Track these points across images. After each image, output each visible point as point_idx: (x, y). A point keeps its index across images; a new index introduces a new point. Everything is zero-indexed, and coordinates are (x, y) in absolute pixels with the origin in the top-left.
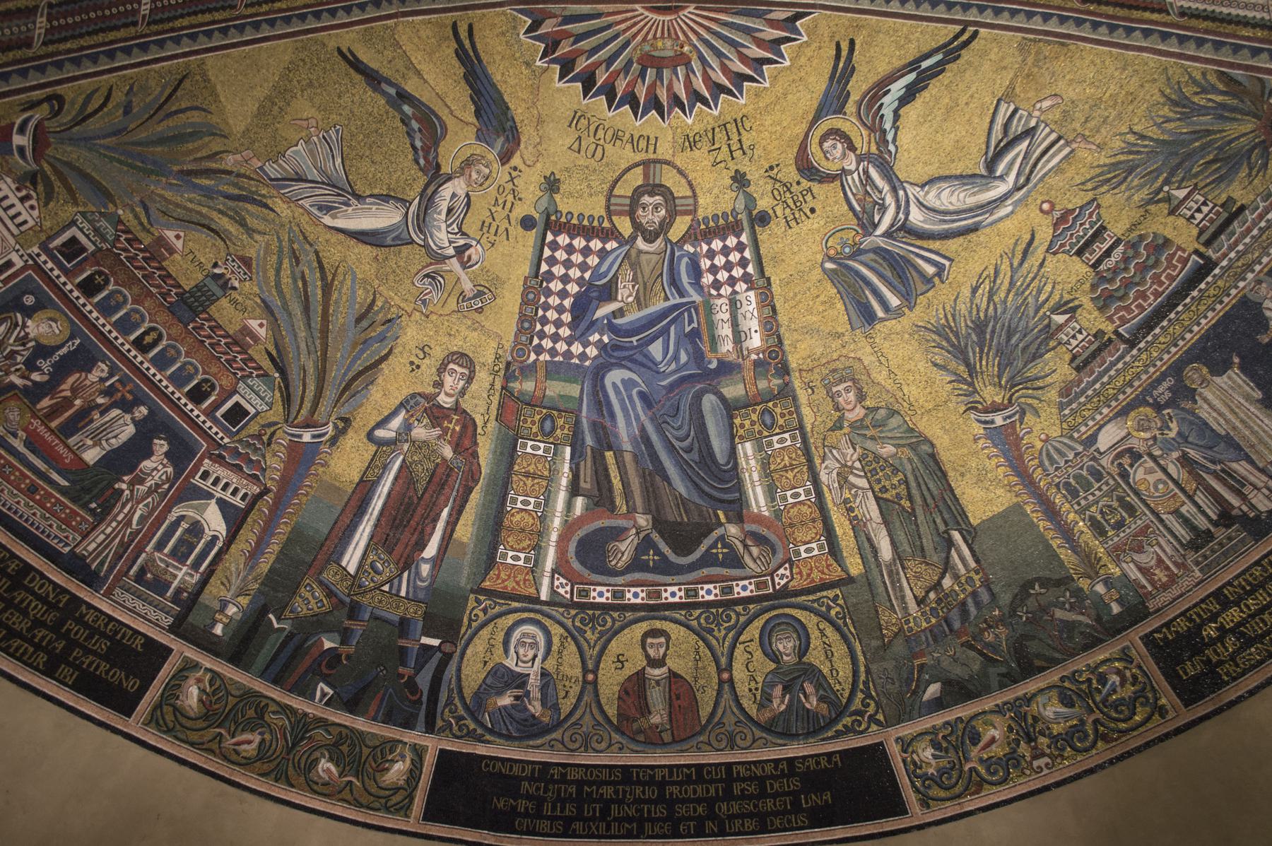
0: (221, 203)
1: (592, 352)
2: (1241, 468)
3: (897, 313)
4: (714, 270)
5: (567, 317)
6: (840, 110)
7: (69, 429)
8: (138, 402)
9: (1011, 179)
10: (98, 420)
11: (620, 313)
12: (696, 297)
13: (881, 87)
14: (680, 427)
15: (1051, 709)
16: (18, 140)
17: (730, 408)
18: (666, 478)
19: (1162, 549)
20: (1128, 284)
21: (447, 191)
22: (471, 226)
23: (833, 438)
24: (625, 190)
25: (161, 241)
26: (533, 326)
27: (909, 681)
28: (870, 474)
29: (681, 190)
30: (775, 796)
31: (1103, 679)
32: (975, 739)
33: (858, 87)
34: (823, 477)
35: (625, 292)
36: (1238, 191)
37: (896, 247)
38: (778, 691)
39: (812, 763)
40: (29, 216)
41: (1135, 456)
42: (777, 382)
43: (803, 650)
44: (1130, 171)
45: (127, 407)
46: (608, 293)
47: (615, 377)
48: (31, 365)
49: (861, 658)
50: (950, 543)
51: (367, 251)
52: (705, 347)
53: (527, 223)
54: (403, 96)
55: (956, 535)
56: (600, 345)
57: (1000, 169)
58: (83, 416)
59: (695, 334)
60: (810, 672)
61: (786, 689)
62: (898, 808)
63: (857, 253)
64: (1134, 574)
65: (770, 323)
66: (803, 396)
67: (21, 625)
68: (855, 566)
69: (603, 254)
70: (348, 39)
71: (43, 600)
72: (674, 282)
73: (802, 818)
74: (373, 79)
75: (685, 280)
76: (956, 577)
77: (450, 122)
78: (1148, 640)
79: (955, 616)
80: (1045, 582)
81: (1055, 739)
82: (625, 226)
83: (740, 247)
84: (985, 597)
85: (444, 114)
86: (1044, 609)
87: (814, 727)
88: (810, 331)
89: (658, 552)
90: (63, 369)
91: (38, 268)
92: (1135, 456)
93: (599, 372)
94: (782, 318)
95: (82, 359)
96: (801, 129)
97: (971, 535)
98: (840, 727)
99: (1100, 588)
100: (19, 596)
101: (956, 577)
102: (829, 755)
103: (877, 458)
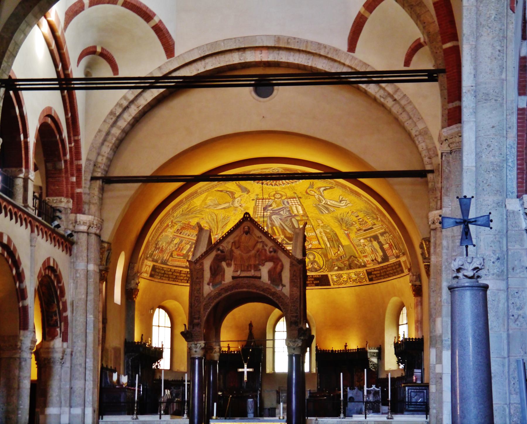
0: (198, 213)
1: (268, 214)
2: (377, 254)
3: (327, 214)
4: (291, 203)
5: (262, 210)
6: (313, 188)
7: (181, 251)
8: (189, 242)
9: (344, 204)
10: (184, 247)
11: (274, 208)
12: (288, 206)
13: (319, 188)
14: (288, 222)
15: (353, 276)
16: (169, 224)
17: (298, 221)
18: (286, 230)
19: (369, 259)
20: (363, 224)
21: (237, 200)
22: (242, 202)
23: (318, 227)
24: (273, 194)
25: (189, 222)
26: (256, 211)
27: (332, 266)
28: (325, 234)
29: (283, 193)
30: (309, 281)
31: (360, 273)
32: (342, 277)
33: (315, 187)
34: (317, 232)
35: (274, 205)
36: (375, 221)
37: (326, 206)
38: (310, 264)
39: (316, 276)
40: (172, 231)
41: (366, 246)
42: (306, 218)
43: (314, 258)
44: (361, 211)
45: (188, 244)
46: (271, 206)
47: (273, 217)
48: (175, 246)
49: (325, 261)
50: (339, 247)
51: (223, 210)
52: (292, 213)
53: (253, 200)
54: (227, 191)
55: (340, 246)
56: (271, 213)
57: (342, 202)
58: (183, 248)
59: (289, 211)
60: (315, 261)
61: (312, 264)
62: (330, 285)
63: (319, 205)
64: (365, 261)
65: (304, 210)
66: (312, 221)
67: (182, 278)
68: (323, 246)
69: (269, 201)
70: (216, 189)
71: (184, 274)
72: (284, 203)
73: (314, 285)
74: (221, 191)
75: (286, 203)
76: (340, 252)
77: (236, 192)
78: (366, 270)
79: (340, 258)
80: (354, 257)
81: (353, 280)
82: (273, 198)
83: (297, 200)
84: (345, 256)
85: (235, 191)
86: (353, 261)
87: (316, 270)
88: (312, 213)
89: (285, 241)
90: (179, 244)
91: (174, 235)
92: (366, 246)
93: (270, 217)
94: (306, 210)
95: (181, 241)
96: (306, 189)
97: (342, 246)
98: (321, 271)
99: (361, 261)
100: (181, 274)
101: (340, 252)
102: (319, 275)
103: (326, 232)
